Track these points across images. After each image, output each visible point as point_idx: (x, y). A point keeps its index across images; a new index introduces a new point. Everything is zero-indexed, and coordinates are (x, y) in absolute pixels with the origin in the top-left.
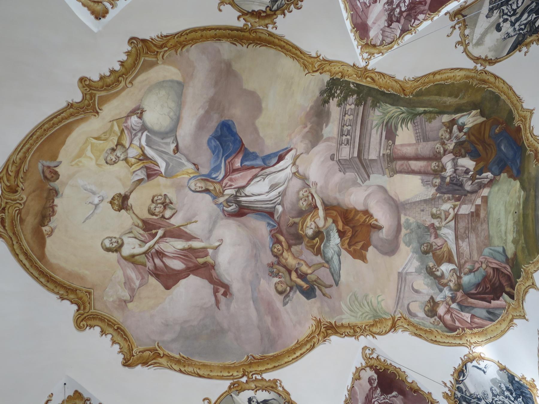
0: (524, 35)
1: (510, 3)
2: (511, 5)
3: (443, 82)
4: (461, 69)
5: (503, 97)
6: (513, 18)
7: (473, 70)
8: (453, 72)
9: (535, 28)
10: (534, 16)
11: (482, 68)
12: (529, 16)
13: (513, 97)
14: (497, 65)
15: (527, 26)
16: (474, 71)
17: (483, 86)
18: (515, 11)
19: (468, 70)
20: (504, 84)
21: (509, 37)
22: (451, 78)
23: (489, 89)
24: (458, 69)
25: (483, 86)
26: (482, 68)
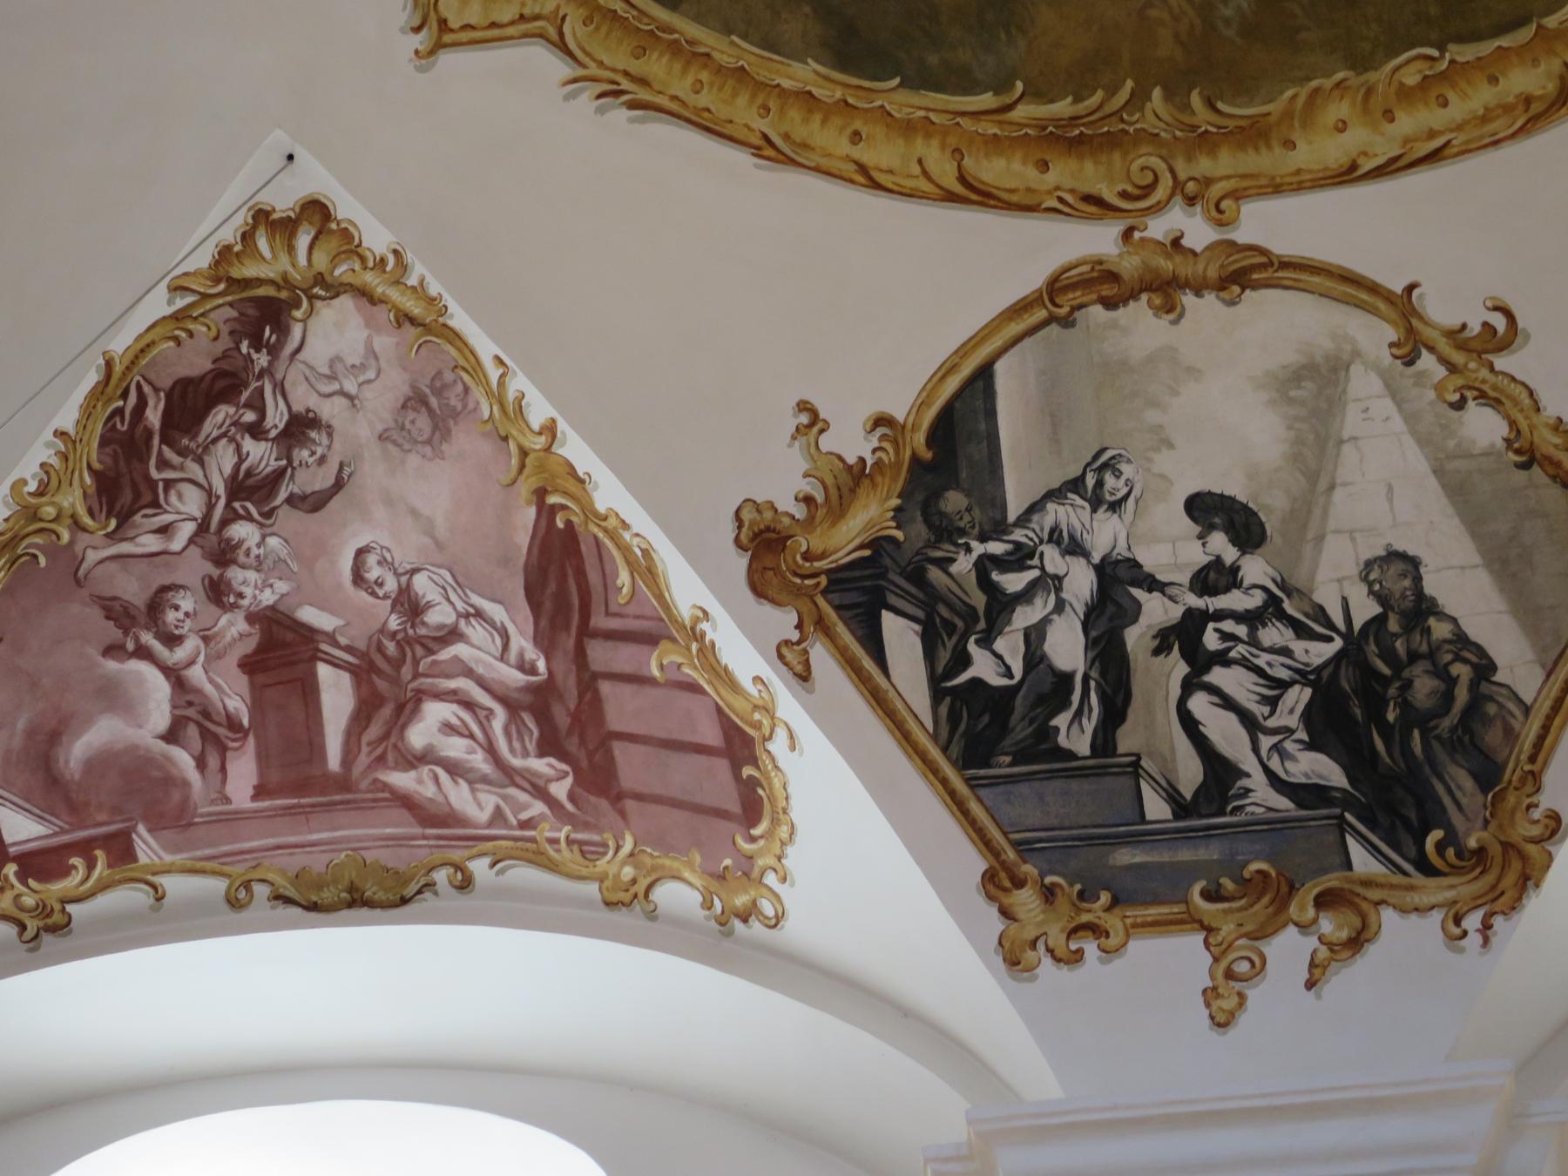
0: (946, 532)
1: (1298, 697)
2: (1283, 685)
3: (1465, 53)
4: (1348, 174)
5: (804, 73)
6: (1157, 611)
7: (1237, 195)
8: (1406, 141)
9: (892, 600)
10: (983, 667)
11: (1158, 228)
12: (1035, 657)
13: (704, 100)
14: (1033, 279)
15: (979, 600)
16: (1216, 190)
17: (1063, 107)
18: (1200, 662)
19: (1276, 188)
20: (862, 169)
21: (1076, 485)
22: (1406, 95)
23: (987, 100)
24: (1379, 172)
25: (1063, 107)
26: (1158, 228)
